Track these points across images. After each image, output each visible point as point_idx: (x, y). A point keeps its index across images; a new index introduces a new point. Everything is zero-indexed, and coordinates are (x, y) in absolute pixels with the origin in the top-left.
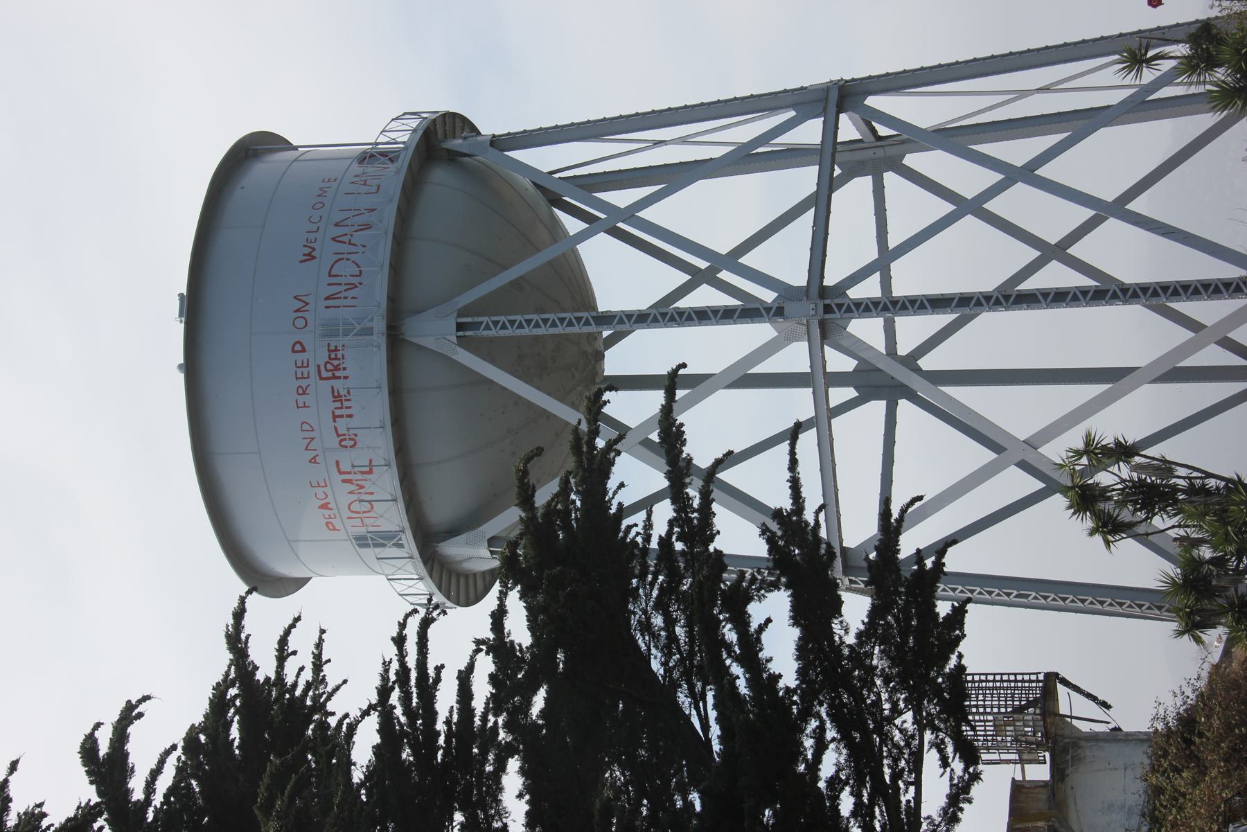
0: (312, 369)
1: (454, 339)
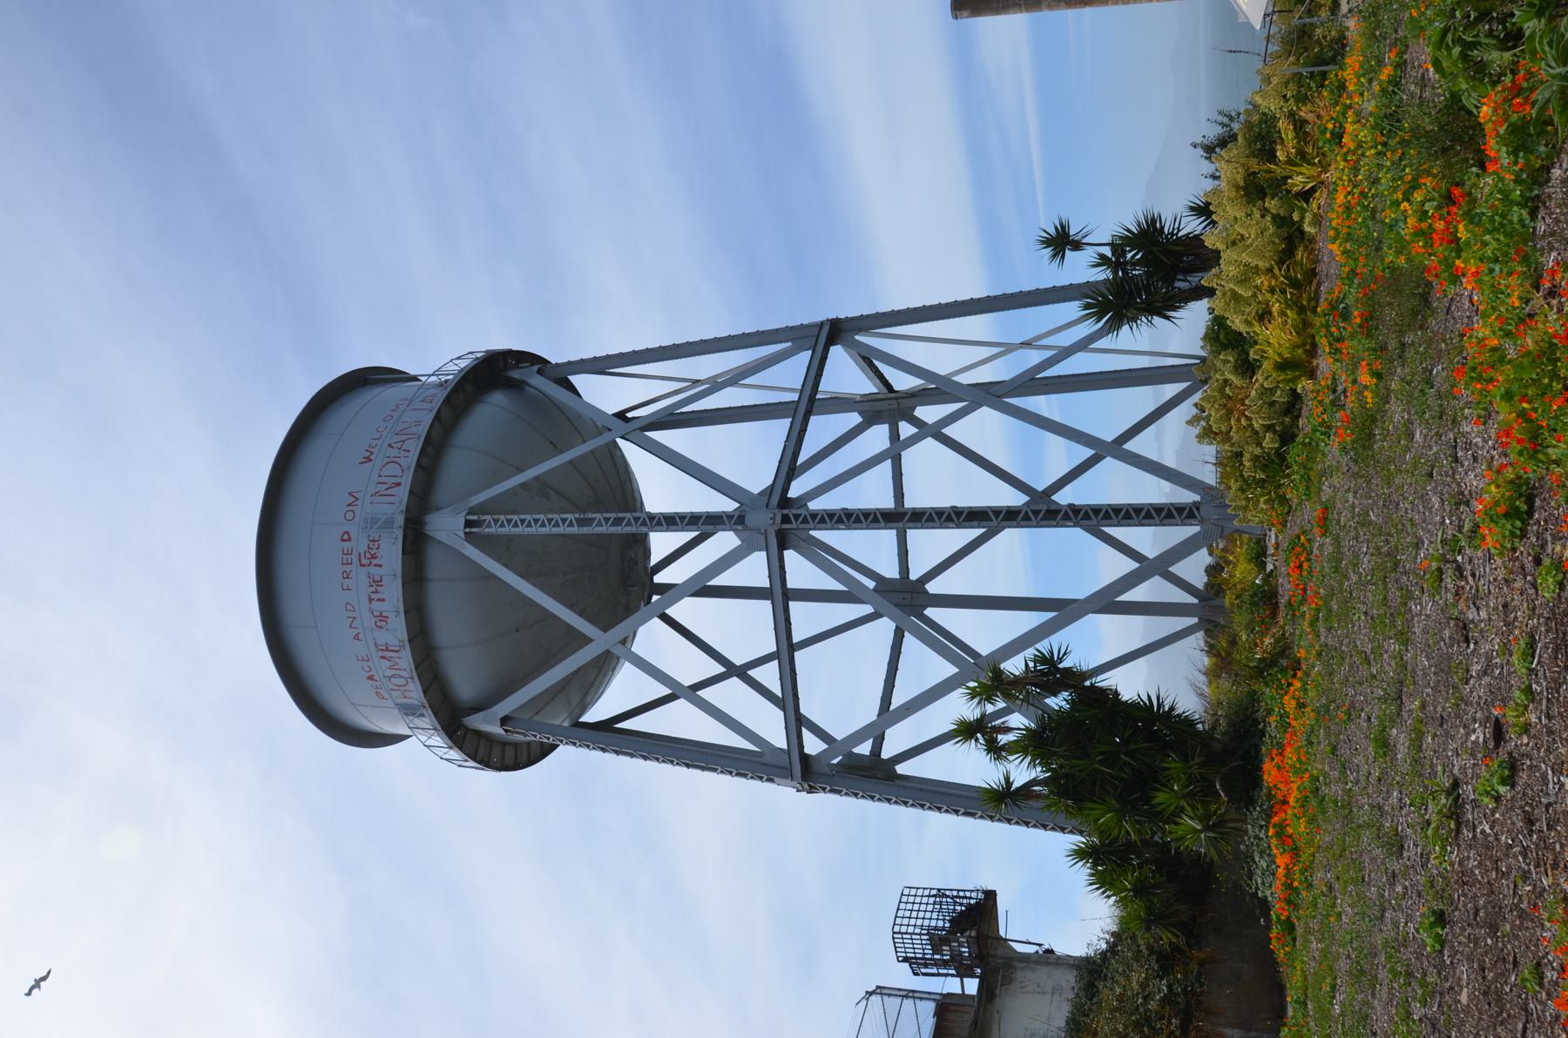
0: (354, 557)
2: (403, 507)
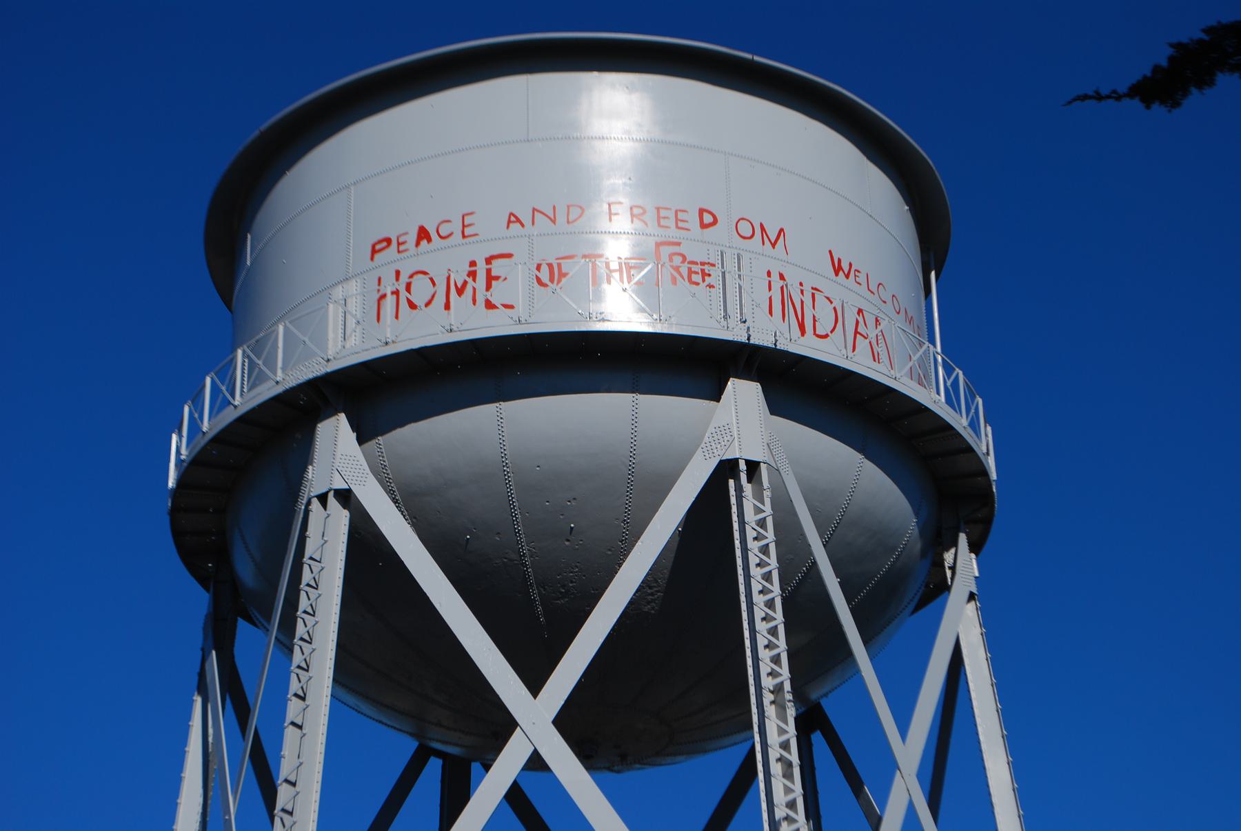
0: (673, 234)
1: (729, 456)
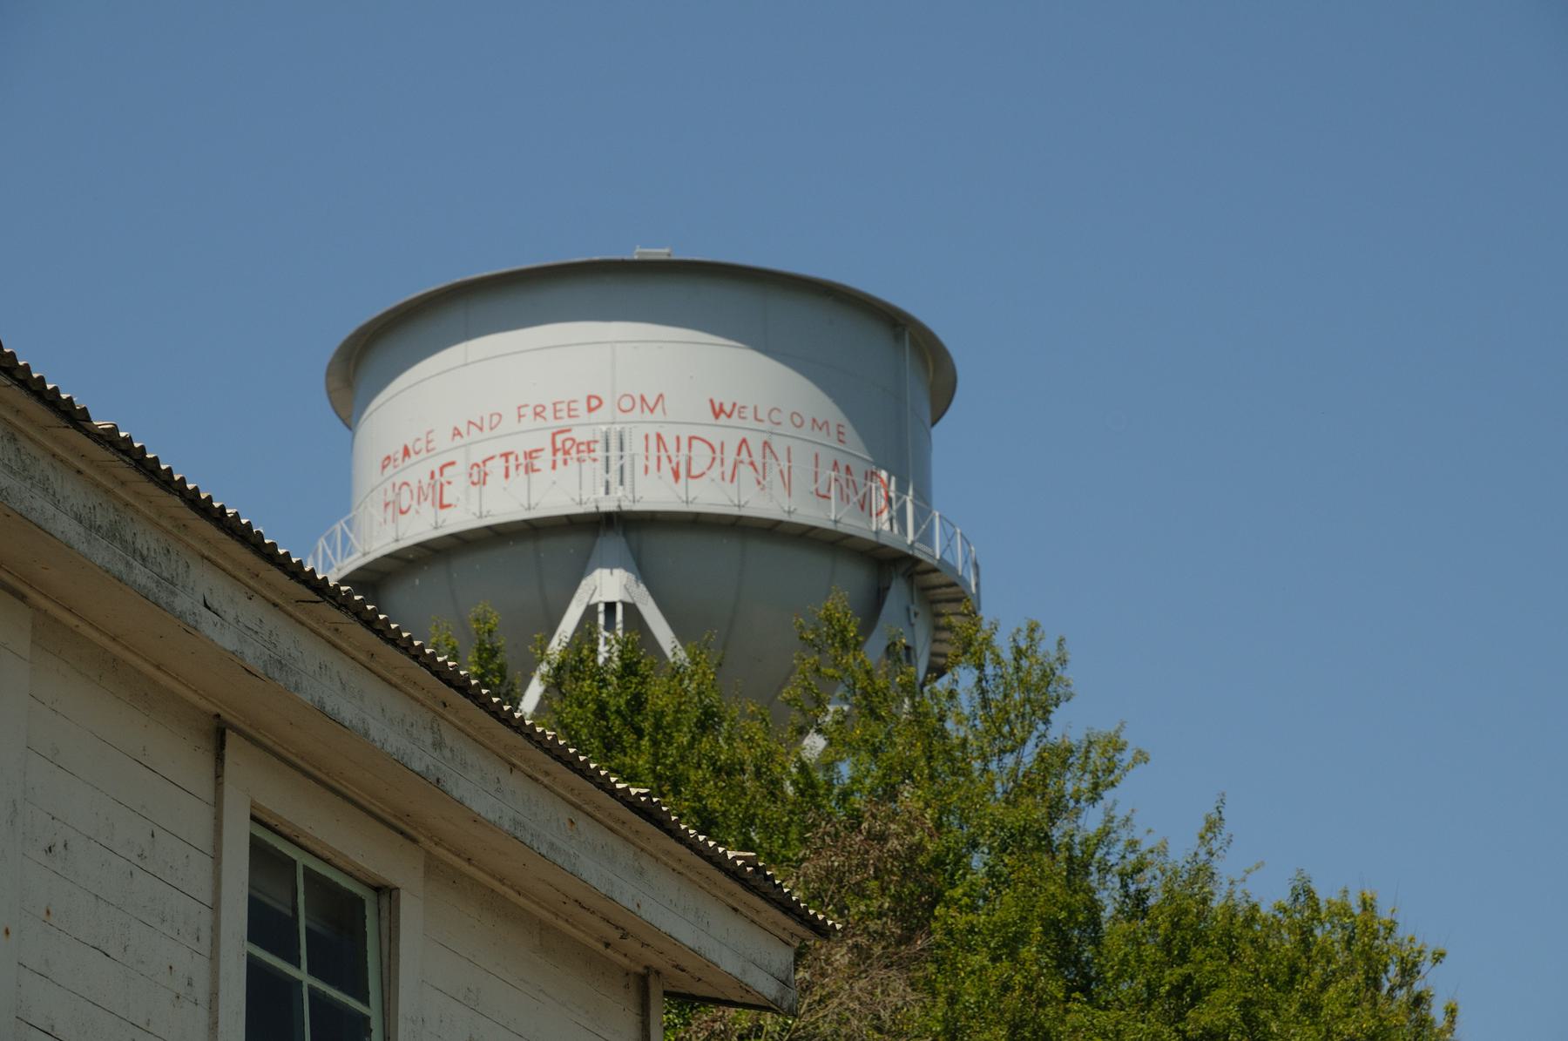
0: (565, 422)
2: (627, 506)
